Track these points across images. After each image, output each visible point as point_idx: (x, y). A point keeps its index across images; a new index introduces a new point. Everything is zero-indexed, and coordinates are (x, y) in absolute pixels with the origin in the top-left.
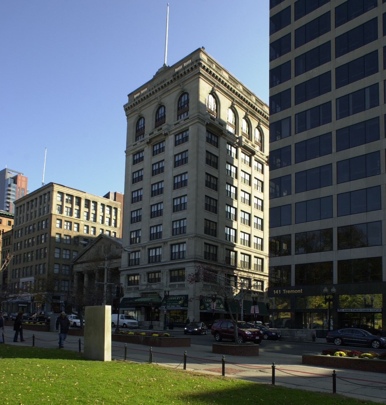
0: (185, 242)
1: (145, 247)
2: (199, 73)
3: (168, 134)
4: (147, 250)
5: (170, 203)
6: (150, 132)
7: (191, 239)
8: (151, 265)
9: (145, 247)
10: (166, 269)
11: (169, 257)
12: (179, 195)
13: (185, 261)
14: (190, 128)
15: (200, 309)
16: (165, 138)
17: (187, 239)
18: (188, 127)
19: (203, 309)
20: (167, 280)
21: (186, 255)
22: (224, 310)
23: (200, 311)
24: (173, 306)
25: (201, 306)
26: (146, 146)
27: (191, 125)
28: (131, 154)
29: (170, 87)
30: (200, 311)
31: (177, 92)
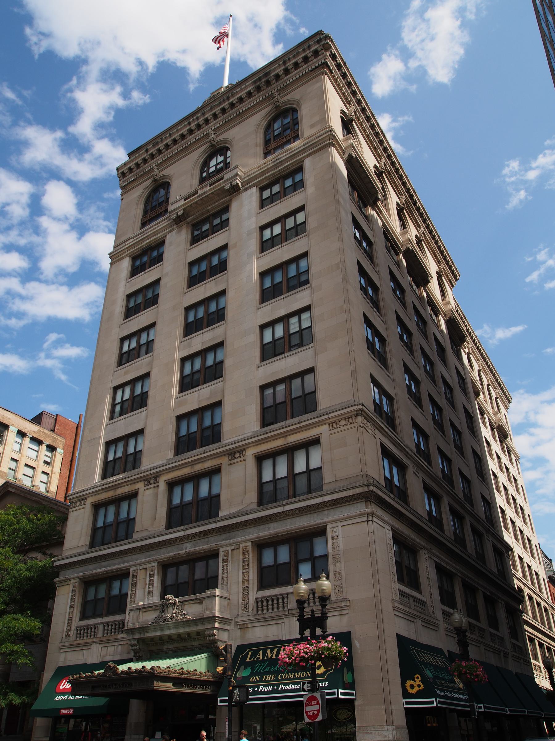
0: (316, 441)
1: (157, 477)
2: (323, 64)
3: (239, 189)
4: (162, 486)
5: (254, 337)
6: (186, 192)
7: (343, 423)
8: (181, 534)
9: (157, 477)
10: (239, 539)
11: (252, 497)
12: (282, 313)
13: (326, 499)
14: (307, 163)
15: (406, 695)
16: (230, 201)
17: (325, 428)
18: (302, 161)
19: (419, 695)
20: (246, 580)
21: (327, 477)
22: (464, 697)
23: (403, 703)
24: (293, 687)
25: (409, 683)
26: (173, 230)
27: (308, 156)
28: (127, 255)
29: (243, 107)
30: (403, 703)
31: (264, 112)
